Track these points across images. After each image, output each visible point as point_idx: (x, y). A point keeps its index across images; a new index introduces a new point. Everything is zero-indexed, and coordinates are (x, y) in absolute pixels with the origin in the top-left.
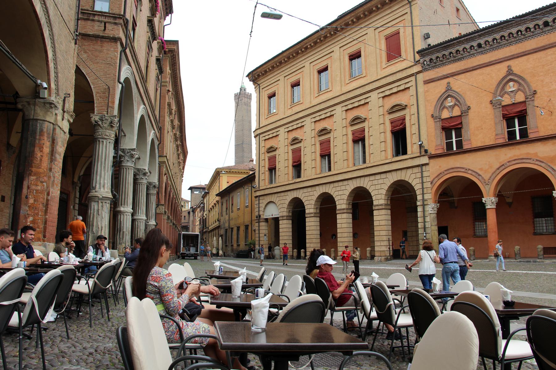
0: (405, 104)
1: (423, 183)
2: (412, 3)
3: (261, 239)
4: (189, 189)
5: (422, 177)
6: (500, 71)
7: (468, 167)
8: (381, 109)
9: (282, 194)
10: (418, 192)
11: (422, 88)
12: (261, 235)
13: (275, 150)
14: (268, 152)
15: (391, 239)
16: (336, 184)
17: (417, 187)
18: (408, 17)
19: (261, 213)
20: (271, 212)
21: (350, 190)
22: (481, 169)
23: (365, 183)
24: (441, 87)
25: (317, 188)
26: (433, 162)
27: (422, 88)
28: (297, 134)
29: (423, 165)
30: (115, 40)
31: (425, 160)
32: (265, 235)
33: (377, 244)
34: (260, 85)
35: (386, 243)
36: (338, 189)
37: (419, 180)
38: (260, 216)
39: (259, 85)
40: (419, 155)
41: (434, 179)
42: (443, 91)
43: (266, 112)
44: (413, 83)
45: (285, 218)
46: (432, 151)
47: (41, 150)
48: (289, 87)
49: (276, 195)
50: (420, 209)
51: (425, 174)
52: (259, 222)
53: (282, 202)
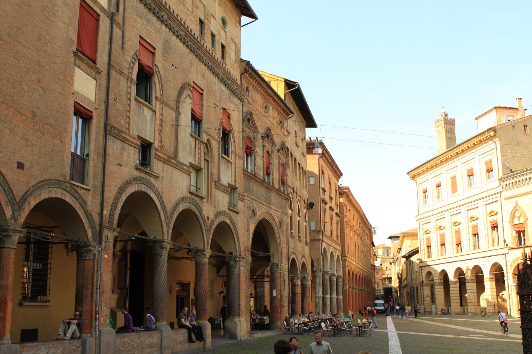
3: (425, 299)
12: (425, 296)
17: (504, 268)
24: (511, 203)
29: (506, 254)
30: (319, 240)
31: (506, 250)
32: (428, 296)
34: (417, 181)
37: (505, 263)
38: (423, 282)
40: (503, 247)
41: (512, 263)
42: (515, 206)
44: (498, 199)
46: (511, 246)
47: (307, 291)
48: (435, 187)
52: (423, 286)
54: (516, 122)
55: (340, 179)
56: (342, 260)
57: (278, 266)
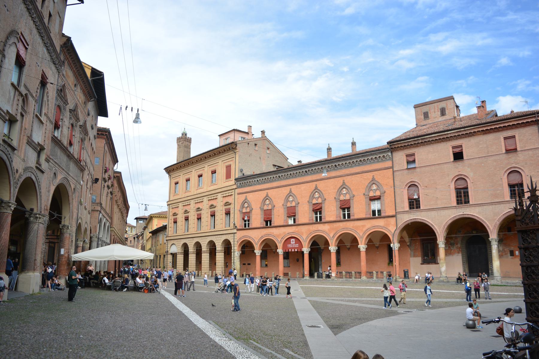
0: (230, 202)
1: (234, 241)
2: (236, 153)
3: (168, 264)
4: (135, 219)
5: (234, 239)
6: (263, 194)
7: (250, 236)
8: (222, 203)
9: (179, 240)
10: (232, 246)
11: (236, 196)
13: (177, 215)
14: (174, 216)
15: (223, 267)
16: (202, 238)
17: (232, 243)
18: (234, 158)
19: (168, 250)
20: (174, 249)
21: (208, 242)
22: (255, 237)
23: (213, 239)
24: (243, 197)
25: (194, 238)
26: (238, 232)
27: (236, 196)
28: (186, 208)
29: (235, 233)
31: (235, 231)
32: (170, 262)
33: (217, 269)
35: (221, 269)
36: (203, 240)
37: (233, 240)
38: (168, 252)
39: (170, 175)
40: (233, 228)
42: (244, 199)
43: (174, 192)
45: (180, 253)
46: (238, 227)
49: (176, 240)
50: (233, 254)
51: (235, 237)
53: (179, 244)
54: (250, 140)
55: (116, 165)
56: (111, 230)
57: (68, 227)
